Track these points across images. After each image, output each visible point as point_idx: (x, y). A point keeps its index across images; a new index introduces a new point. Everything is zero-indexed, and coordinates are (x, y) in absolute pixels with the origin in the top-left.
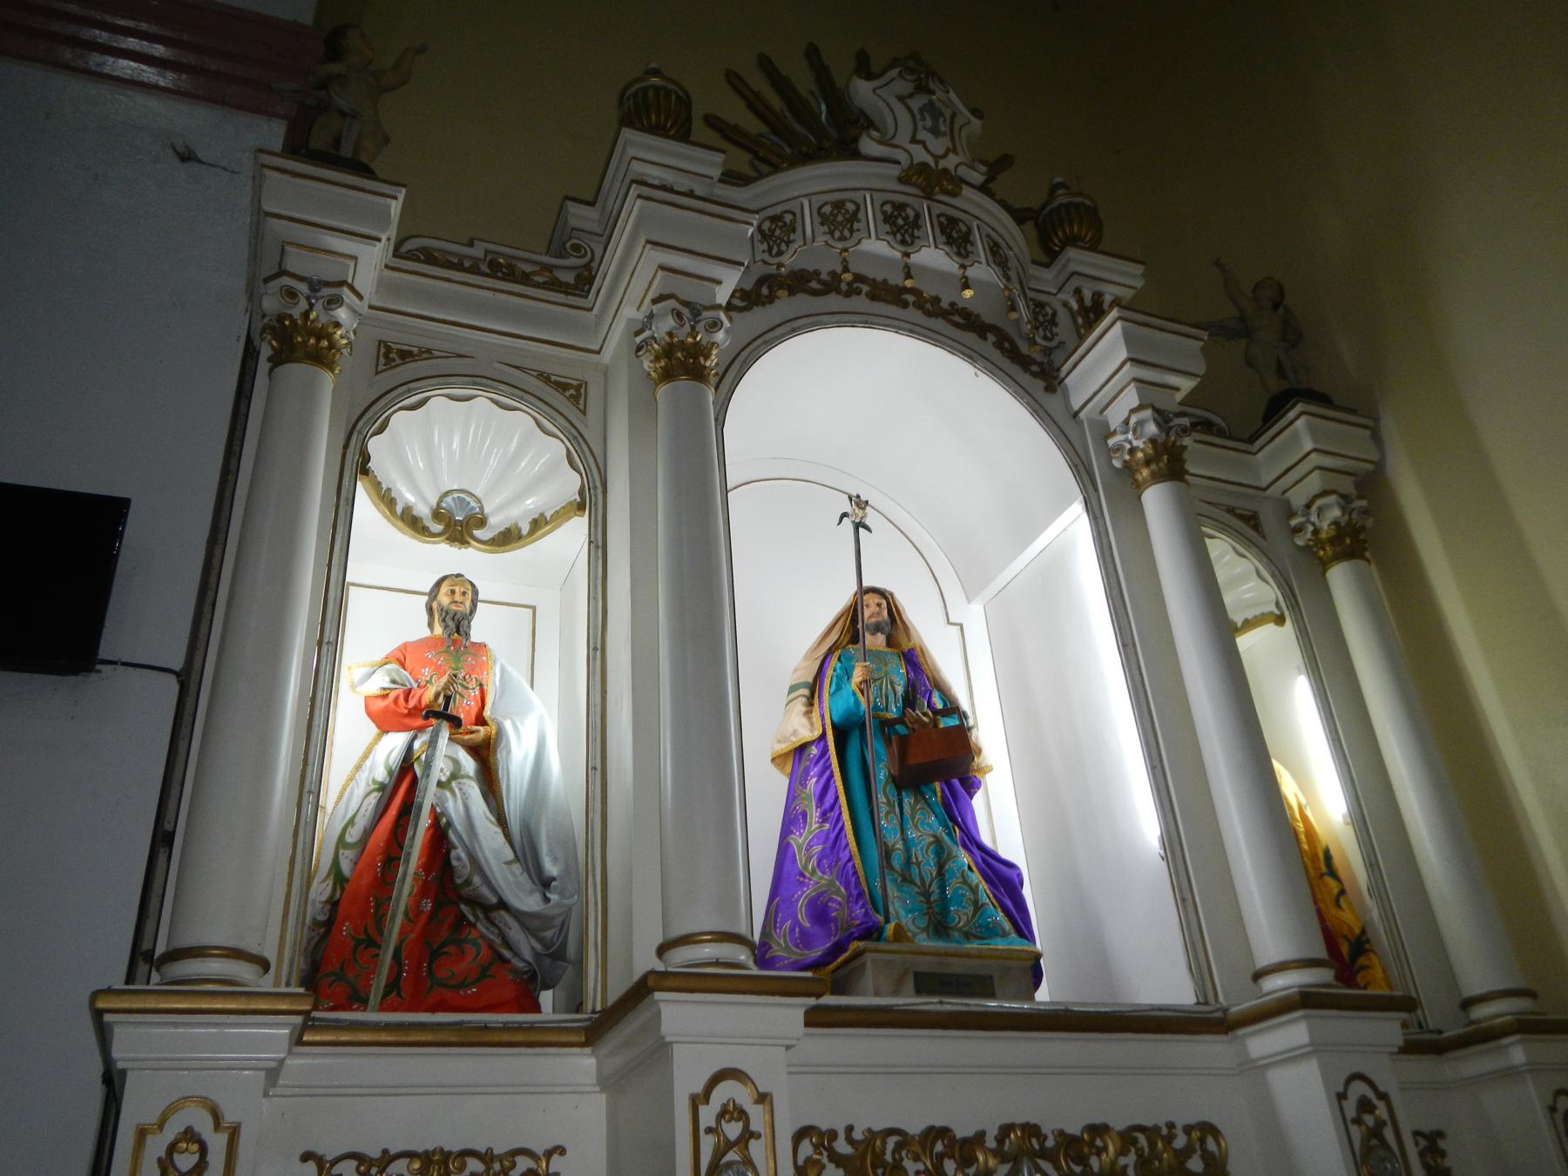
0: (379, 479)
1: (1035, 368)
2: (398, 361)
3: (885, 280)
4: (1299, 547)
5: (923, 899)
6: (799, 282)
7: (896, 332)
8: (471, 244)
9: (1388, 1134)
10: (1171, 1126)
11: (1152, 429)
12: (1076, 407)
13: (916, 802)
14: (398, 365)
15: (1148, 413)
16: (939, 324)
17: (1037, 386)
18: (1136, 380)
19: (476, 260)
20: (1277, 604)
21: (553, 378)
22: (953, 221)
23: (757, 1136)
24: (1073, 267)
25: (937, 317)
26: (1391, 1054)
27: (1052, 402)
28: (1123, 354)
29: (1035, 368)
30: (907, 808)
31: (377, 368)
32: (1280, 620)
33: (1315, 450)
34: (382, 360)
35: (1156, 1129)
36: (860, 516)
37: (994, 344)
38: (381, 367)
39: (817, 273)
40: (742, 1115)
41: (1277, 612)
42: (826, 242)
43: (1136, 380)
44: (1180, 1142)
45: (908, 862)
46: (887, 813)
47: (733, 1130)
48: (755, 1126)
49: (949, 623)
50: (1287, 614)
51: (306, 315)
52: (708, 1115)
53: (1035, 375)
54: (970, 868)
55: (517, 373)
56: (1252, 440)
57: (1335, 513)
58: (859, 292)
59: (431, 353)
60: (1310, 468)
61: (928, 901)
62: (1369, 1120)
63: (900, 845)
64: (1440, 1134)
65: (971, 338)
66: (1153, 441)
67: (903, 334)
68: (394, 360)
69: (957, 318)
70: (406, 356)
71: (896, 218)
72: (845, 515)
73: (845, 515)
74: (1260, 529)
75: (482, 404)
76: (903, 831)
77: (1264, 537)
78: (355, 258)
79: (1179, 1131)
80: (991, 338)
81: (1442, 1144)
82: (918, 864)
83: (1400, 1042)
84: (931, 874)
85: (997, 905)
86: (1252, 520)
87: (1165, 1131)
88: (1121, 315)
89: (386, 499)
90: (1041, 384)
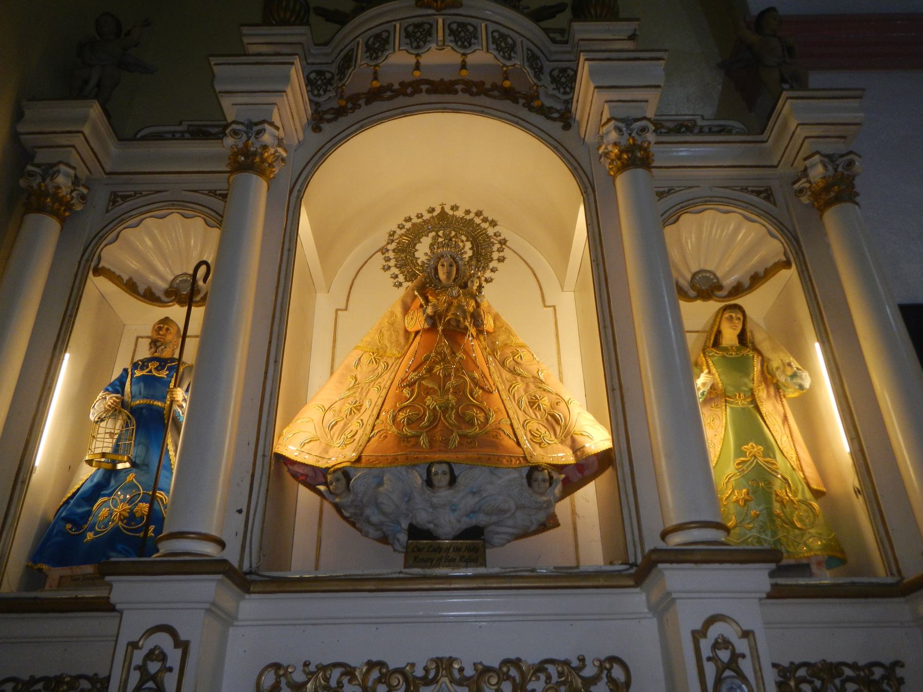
0: (118, 273)
1: (556, 115)
2: (120, 202)
3: (442, 80)
4: (806, 205)
6: (375, 95)
8: (180, 124)
9: (746, 665)
12: (583, 136)
14: (120, 205)
16: (483, 100)
17: (555, 128)
18: (607, 102)
19: (183, 133)
20: (785, 254)
21: (218, 192)
22: (462, 25)
23: (170, 670)
24: (578, 36)
25: (480, 95)
26: (760, 599)
27: (567, 137)
28: (592, 86)
29: (556, 115)
31: (108, 209)
32: (787, 264)
33: (799, 125)
34: (111, 204)
35: (566, 663)
37: (523, 105)
38: (110, 208)
39: (389, 87)
40: (163, 657)
41: (784, 259)
42: (368, 65)
43: (607, 102)
44: (589, 672)
47: (154, 667)
48: (168, 664)
49: (545, 306)
50: (792, 259)
51: (39, 185)
52: (138, 657)
53: (554, 119)
55: (194, 194)
56: (762, 133)
57: (820, 169)
58: (421, 91)
59: (141, 194)
60: (800, 141)
62: (724, 655)
64: (897, 664)
65: (508, 105)
68: (118, 201)
69: (496, 93)
70: (125, 198)
71: (416, 33)
74: (771, 199)
75: (175, 218)
77: (775, 204)
78: (73, 146)
79: (588, 662)
80: (522, 101)
81: (899, 672)
83: (767, 588)
86: (767, 194)
87: (575, 663)
88: (586, 57)
89: (131, 287)
90: (559, 125)
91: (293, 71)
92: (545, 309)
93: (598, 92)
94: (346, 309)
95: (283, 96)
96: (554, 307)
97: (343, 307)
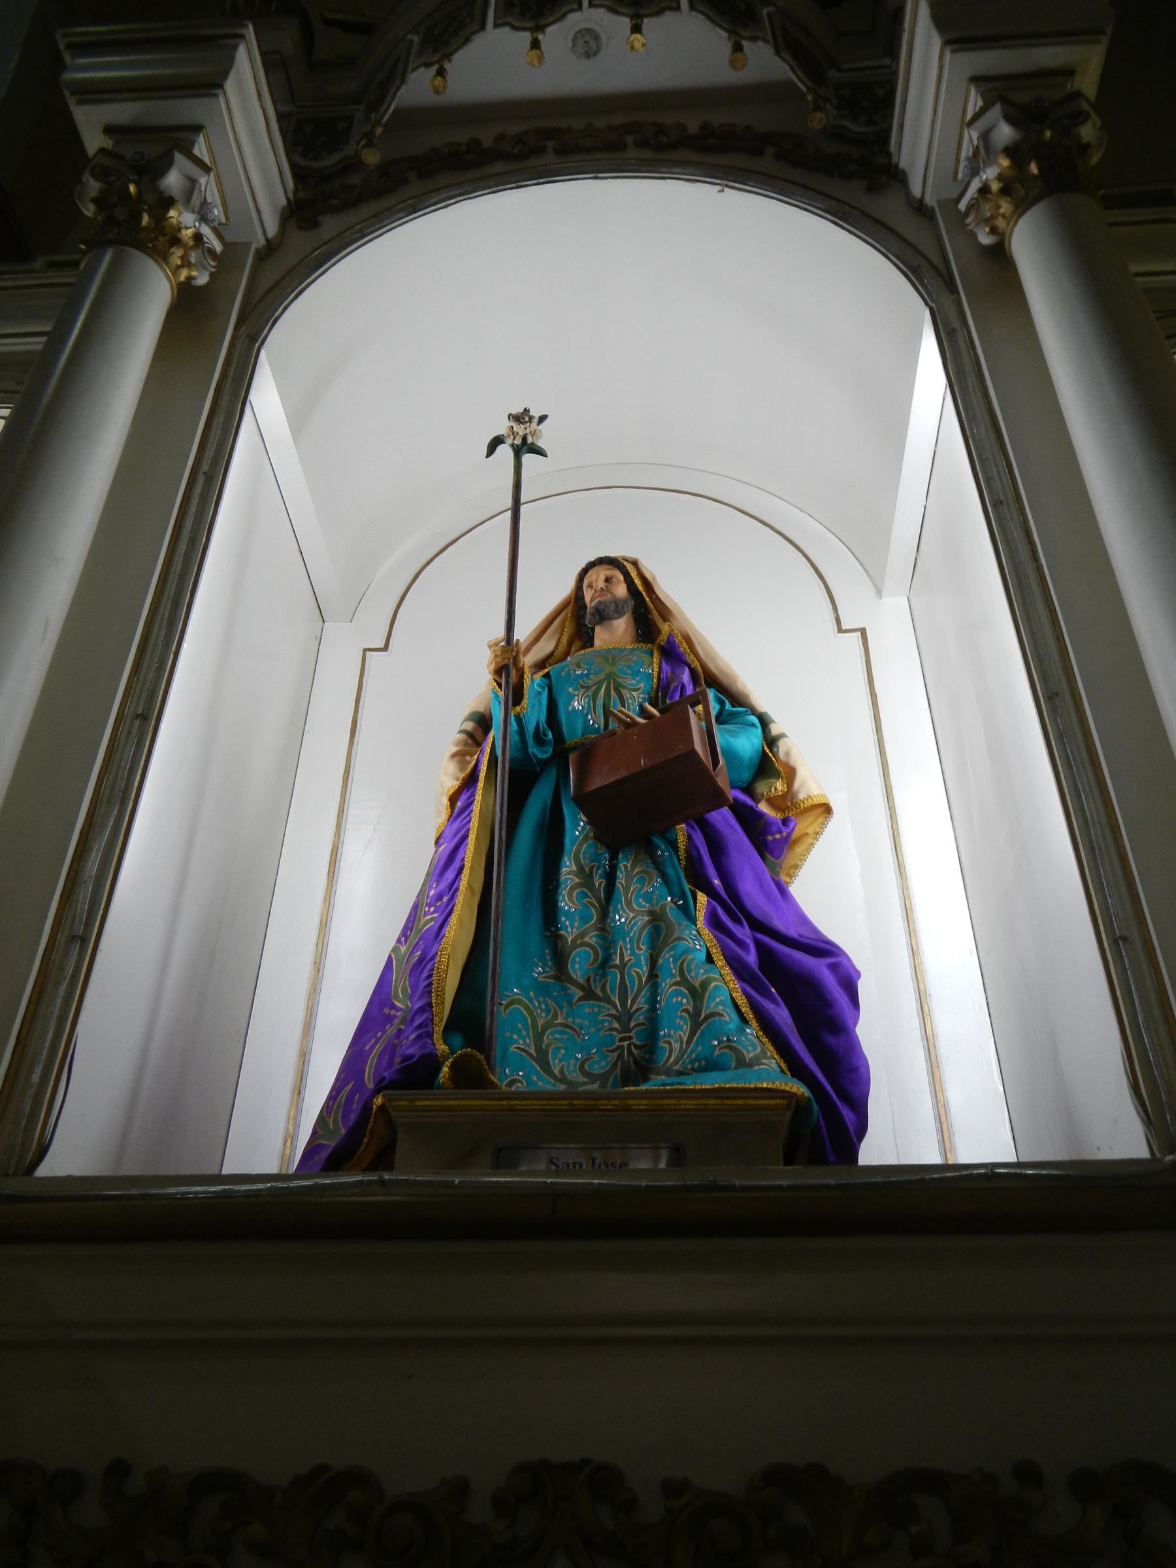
5: (617, 1025)
7: (597, 178)
10: (1028, 1473)
11: (1005, 133)
13: (633, 867)
15: (997, 110)
28: (937, 42)
30: (621, 876)
36: (521, 433)
45: (604, 964)
46: (573, 888)
49: (840, 630)
54: (709, 959)
61: (626, 1028)
63: (592, 938)
66: (1011, 151)
67: (606, 178)
72: (496, 442)
73: (496, 442)
76: (604, 914)
82: (622, 967)
84: (640, 979)
85: (750, 1016)
91: (241, 53)
92: (840, 634)
93: (953, 51)
94: (385, 648)
95: (216, 96)
96: (863, 632)
97: (382, 645)
